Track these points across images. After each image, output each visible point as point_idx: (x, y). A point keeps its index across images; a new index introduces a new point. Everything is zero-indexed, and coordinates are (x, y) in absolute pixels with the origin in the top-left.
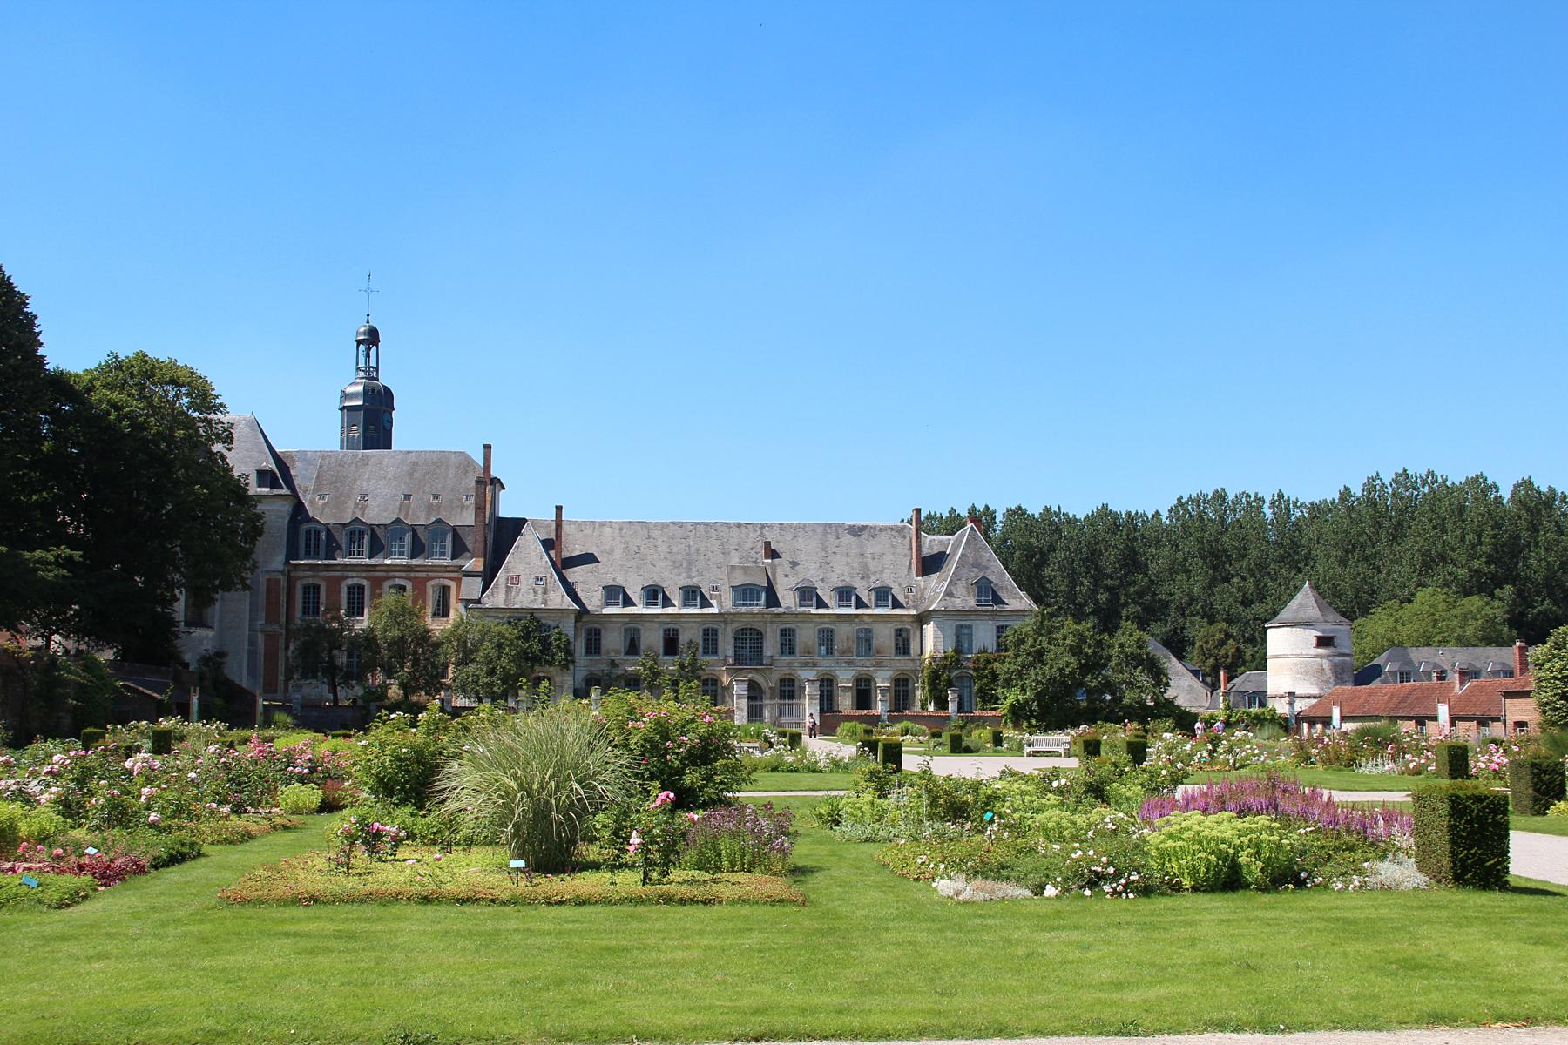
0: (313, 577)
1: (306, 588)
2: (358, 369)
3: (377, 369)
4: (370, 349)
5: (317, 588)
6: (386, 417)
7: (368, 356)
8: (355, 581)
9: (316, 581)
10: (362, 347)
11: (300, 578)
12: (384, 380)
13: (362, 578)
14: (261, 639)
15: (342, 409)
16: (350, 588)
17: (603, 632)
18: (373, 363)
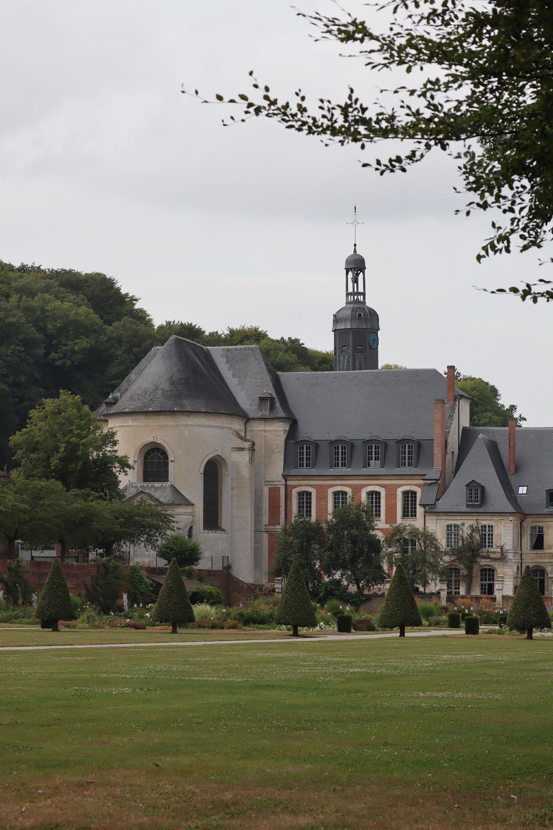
0: (306, 485)
1: (300, 494)
2: (348, 294)
3: (364, 294)
4: (358, 275)
5: (309, 494)
6: (372, 337)
7: (355, 281)
8: (339, 489)
9: (309, 489)
10: (350, 275)
11: (295, 487)
12: (370, 303)
13: (344, 485)
14: (265, 536)
15: (334, 331)
16: (336, 494)
17: (545, 530)
18: (361, 290)
